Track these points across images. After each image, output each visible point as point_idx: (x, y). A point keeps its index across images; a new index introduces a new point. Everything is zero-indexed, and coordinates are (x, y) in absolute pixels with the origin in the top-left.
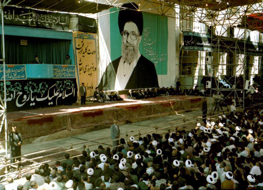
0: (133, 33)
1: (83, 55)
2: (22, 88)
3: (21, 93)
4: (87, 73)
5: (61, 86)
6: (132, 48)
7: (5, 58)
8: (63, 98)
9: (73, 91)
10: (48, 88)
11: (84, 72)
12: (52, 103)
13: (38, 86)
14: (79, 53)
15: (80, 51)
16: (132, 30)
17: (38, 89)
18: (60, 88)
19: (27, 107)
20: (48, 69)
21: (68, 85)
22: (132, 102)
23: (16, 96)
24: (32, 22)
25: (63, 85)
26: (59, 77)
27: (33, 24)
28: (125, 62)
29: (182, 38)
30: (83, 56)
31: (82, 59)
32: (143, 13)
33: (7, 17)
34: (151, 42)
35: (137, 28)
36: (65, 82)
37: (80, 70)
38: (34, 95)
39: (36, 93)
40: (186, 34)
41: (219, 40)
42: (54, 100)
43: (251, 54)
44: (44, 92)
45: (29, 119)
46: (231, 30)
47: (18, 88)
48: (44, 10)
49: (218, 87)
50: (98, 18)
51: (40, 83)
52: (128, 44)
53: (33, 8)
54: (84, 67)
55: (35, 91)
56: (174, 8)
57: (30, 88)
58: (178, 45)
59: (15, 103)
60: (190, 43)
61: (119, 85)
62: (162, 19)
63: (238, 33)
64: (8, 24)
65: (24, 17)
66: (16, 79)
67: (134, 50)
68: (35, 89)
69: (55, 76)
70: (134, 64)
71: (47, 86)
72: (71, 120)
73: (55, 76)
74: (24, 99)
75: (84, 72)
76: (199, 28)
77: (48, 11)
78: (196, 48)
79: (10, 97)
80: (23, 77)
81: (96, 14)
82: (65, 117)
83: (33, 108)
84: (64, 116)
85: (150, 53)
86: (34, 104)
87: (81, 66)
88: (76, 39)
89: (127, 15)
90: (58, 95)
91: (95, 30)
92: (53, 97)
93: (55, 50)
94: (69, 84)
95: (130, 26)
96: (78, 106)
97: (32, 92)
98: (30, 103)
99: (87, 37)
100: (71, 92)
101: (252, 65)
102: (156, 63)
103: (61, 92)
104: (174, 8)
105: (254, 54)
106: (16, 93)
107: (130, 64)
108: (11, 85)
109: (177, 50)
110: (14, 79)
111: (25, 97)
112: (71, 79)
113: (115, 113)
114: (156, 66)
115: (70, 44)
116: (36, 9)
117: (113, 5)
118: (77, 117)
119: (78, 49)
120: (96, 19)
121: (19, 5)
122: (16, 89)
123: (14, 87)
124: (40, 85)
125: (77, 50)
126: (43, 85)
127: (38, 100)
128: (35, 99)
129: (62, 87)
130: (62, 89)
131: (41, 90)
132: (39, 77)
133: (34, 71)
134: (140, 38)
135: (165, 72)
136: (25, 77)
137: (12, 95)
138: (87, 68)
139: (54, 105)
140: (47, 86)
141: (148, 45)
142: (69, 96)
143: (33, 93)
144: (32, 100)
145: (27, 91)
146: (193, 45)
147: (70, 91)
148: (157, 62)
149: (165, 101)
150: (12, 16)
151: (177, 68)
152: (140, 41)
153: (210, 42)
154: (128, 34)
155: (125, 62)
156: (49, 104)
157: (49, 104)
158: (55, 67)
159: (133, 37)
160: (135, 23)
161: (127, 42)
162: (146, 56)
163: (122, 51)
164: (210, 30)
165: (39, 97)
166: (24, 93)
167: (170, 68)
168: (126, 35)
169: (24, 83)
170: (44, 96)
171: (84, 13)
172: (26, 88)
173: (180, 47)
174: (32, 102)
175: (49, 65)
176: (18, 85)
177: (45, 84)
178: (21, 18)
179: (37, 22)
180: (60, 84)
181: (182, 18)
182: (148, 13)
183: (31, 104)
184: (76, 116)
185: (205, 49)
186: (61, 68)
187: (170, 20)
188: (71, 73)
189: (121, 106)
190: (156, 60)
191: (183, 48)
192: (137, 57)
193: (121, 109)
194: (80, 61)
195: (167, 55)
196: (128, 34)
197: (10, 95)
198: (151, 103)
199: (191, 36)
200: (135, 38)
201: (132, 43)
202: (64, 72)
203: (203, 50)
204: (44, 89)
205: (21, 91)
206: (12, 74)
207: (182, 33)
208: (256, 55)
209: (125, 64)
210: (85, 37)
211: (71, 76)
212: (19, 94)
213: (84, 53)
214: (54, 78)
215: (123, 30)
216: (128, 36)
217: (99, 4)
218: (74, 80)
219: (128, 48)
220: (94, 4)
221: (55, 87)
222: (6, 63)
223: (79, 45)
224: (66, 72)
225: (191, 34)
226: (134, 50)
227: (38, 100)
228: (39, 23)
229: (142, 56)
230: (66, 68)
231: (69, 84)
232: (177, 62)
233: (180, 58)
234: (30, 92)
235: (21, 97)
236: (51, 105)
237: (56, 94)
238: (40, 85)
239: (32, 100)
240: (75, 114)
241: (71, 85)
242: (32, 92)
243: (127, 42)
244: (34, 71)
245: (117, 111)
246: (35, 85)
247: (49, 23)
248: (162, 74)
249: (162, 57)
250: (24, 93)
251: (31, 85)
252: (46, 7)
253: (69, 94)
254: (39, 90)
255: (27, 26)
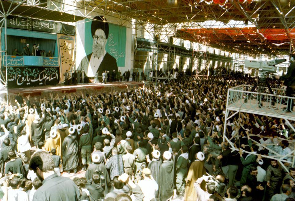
0: (102, 37)
1: (65, 51)
2: (21, 72)
3: (20, 76)
4: (68, 63)
5: (48, 72)
6: (100, 47)
7: (7, 51)
8: (50, 80)
9: (57, 75)
10: (39, 73)
11: (66, 63)
12: (42, 83)
13: (32, 71)
14: (62, 49)
15: (62, 48)
16: (100, 35)
17: (32, 73)
18: (48, 73)
19: (24, 85)
20: (39, 60)
21: (53, 71)
22: (97, 84)
23: (17, 78)
24: (29, 26)
25: (50, 71)
26: (47, 65)
27: (30, 28)
28: (95, 57)
29: (136, 42)
30: (65, 52)
31: (64, 53)
32: (109, 25)
33: (12, 23)
34: (114, 44)
35: (104, 33)
36: (51, 69)
37: (63, 61)
38: (30, 77)
39: (31, 76)
40: (139, 39)
41: (158, 45)
42: (43, 81)
43: (184, 55)
44: (36, 75)
45: (24, 93)
46: (171, 39)
47: (18, 72)
48: (38, 19)
49: (156, 76)
50: (76, 25)
51: (33, 69)
52: (97, 45)
53: (30, 17)
54: (66, 59)
55: (30, 74)
56: (131, 22)
57: (27, 73)
58: (133, 47)
59: (16, 82)
60: (142, 46)
61: (91, 72)
62: (122, 29)
63: (177, 42)
64: (9, 27)
65: (24, 23)
66: (17, 66)
67: (102, 49)
68: (30, 73)
69: (44, 65)
70: (102, 59)
71: (38, 71)
72: (53, 94)
73: (44, 65)
74: (22, 80)
75: (66, 63)
76: (149, 36)
77: (40, 19)
78: (146, 50)
79: (13, 78)
80: (22, 64)
81: (75, 23)
82: (49, 93)
83: (29, 86)
84: (48, 92)
85: (113, 51)
86: (29, 83)
87: (63, 59)
88: (60, 39)
89: (98, 24)
90: (46, 78)
91: (75, 35)
92: (43, 79)
93: (45, 47)
94: (54, 70)
95: (100, 32)
96: (60, 85)
97: (28, 75)
98: (26, 83)
99: (68, 38)
100: (55, 76)
101: (184, 63)
102: (117, 59)
103: (48, 76)
104: (131, 22)
105: (186, 56)
106: (17, 75)
107: (99, 58)
108: (14, 70)
109: (132, 50)
110: (15, 66)
111: (23, 78)
112: (56, 67)
113: (85, 91)
114: (117, 60)
115: (56, 42)
116: (32, 18)
117: (86, 17)
118: (58, 93)
119: (61, 46)
120: (75, 26)
121: (20, 15)
122: (17, 73)
123: (15, 71)
124: (34, 70)
125: (60, 47)
126: (36, 71)
127: (32, 81)
128: (30, 80)
129: (49, 73)
130: (49, 74)
131: (34, 74)
132: (33, 65)
133: (29, 61)
134: (106, 40)
135: (123, 65)
136: (23, 65)
137: (14, 77)
138: (68, 60)
139: (43, 85)
140: (38, 71)
141: (112, 46)
142: (54, 79)
143: (28, 76)
144: (28, 80)
145: (25, 74)
146: (144, 47)
147: (54, 76)
148: (118, 58)
149: (121, 84)
150: (16, 22)
151: (132, 62)
152: (106, 43)
153: (156, 46)
154: (98, 37)
155: (95, 57)
156: (40, 84)
157: (40, 84)
158: (44, 59)
159: (101, 40)
160: (103, 29)
161: (97, 43)
162: (110, 53)
163: (93, 49)
164: (156, 38)
165: (33, 79)
166: (23, 75)
167: (127, 63)
168: (97, 38)
169: (22, 69)
170: (36, 79)
171: (66, 21)
172: (24, 72)
173: (134, 48)
174: (28, 82)
175: (40, 57)
176: (18, 70)
177: (37, 70)
178: (22, 24)
179: (32, 27)
180: (47, 70)
181: (136, 28)
182: (112, 24)
183: (27, 84)
184: (57, 92)
185: (152, 50)
186: (48, 59)
187: (128, 29)
188: (55, 63)
189: (90, 86)
190: (117, 57)
191: (136, 49)
192: (103, 54)
193: (89, 89)
194: (63, 55)
195: (125, 53)
196: (98, 37)
197: (13, 76)
198: (111, 85)
199: (142, 41)
200: (103, 41)
201: (100, 44)
202: (50, 62)
203: (151, 51)
204: (36, 74)
205: (20, 74)
206: (14, 62)
207: (136, 39)
208: (178, 55)
209: (95, 58)
210: (66, 38)
211: (55, 65)
212: (19, 77)
213: (65, 49)
214: (43, 66)
215: (94, 34)
216: (98, 39)
217: (76, 16)
218: (58, 68)
219: (98, 47)
220: (73, 16)
221: (44, 72)
222: (7, 55)
223: (62, 44)
224: (52, 62)
225: (142, 40)
226: (102, 49)
227: (32, 81)
228: (34, 28)
229: (107, 53)
230: (52, 59)
231: (54, 70)
232: (132, 58)
233: (134, 56)
234: (27, 75)
235: (20, 79)
236: (41, 85)
237: (45, 77)
238: (34, 70)
239: (28, 80)
240: (56, 91)
241: (55, 71)
242: (28, 75)
243: (97, 43)
244: (29, 61)
245: (86, 90)
246: (30, 70)
247: (41, 28)
248: (121, 66)
249: (121, 54)
250: (23, 75)
251: (27, 70)
252: (39, 17)
253: (54, 78)
254: (33, 74)
255: (25, 29)
